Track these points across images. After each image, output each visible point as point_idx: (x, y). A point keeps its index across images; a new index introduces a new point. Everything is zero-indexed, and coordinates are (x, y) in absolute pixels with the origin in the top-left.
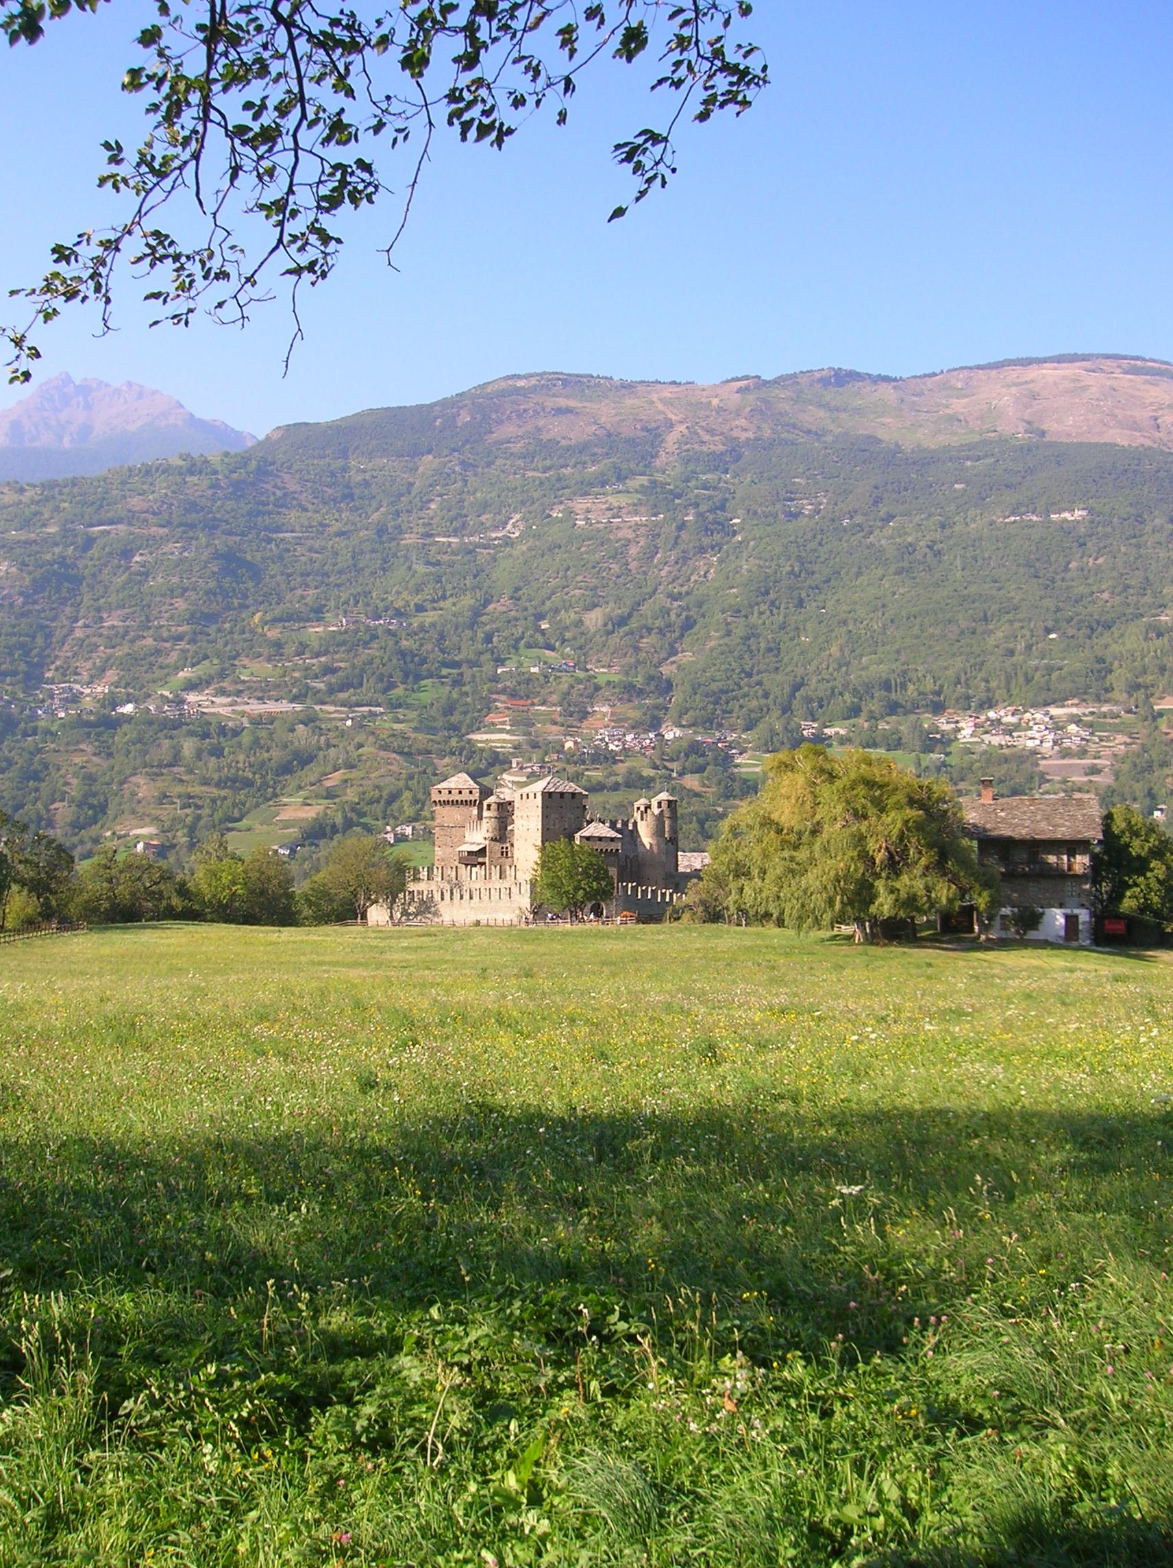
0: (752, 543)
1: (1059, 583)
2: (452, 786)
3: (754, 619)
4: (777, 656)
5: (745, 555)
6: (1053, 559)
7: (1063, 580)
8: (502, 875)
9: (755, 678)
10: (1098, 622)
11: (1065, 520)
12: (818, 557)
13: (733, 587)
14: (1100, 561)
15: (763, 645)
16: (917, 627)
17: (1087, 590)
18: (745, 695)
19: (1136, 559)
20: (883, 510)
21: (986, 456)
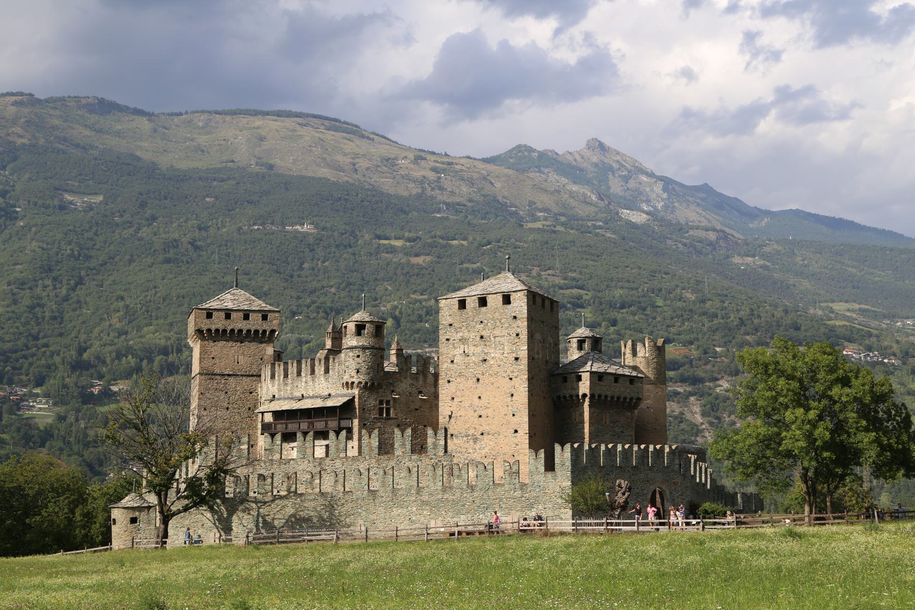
0: (34, 229)
1: (295, 279)
2: (230, 305)
3: (39, 290)
4: (61, 323)
5: (29, 236)
6: (290, 260)
7: (299, 276)
8: (419, 447)
9: (41, 342)
10: (331, 309)
11: (297, 232)
12: (94, 245)
13: (18, 264)
14: (327, 264)
15: (47, 314)
16: (186, 305)
17: (319, 285)
18: (34, 355)
19: (354, 263)
20: (149, 212)
21: (229, 179)
